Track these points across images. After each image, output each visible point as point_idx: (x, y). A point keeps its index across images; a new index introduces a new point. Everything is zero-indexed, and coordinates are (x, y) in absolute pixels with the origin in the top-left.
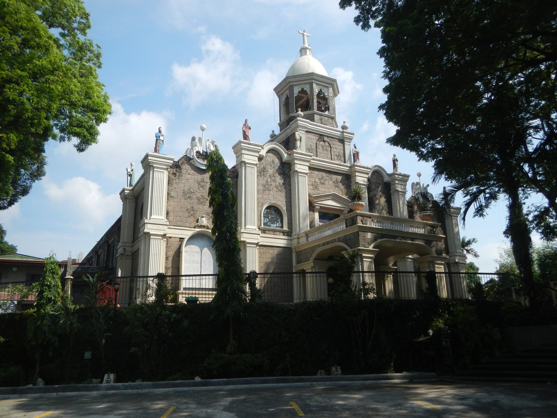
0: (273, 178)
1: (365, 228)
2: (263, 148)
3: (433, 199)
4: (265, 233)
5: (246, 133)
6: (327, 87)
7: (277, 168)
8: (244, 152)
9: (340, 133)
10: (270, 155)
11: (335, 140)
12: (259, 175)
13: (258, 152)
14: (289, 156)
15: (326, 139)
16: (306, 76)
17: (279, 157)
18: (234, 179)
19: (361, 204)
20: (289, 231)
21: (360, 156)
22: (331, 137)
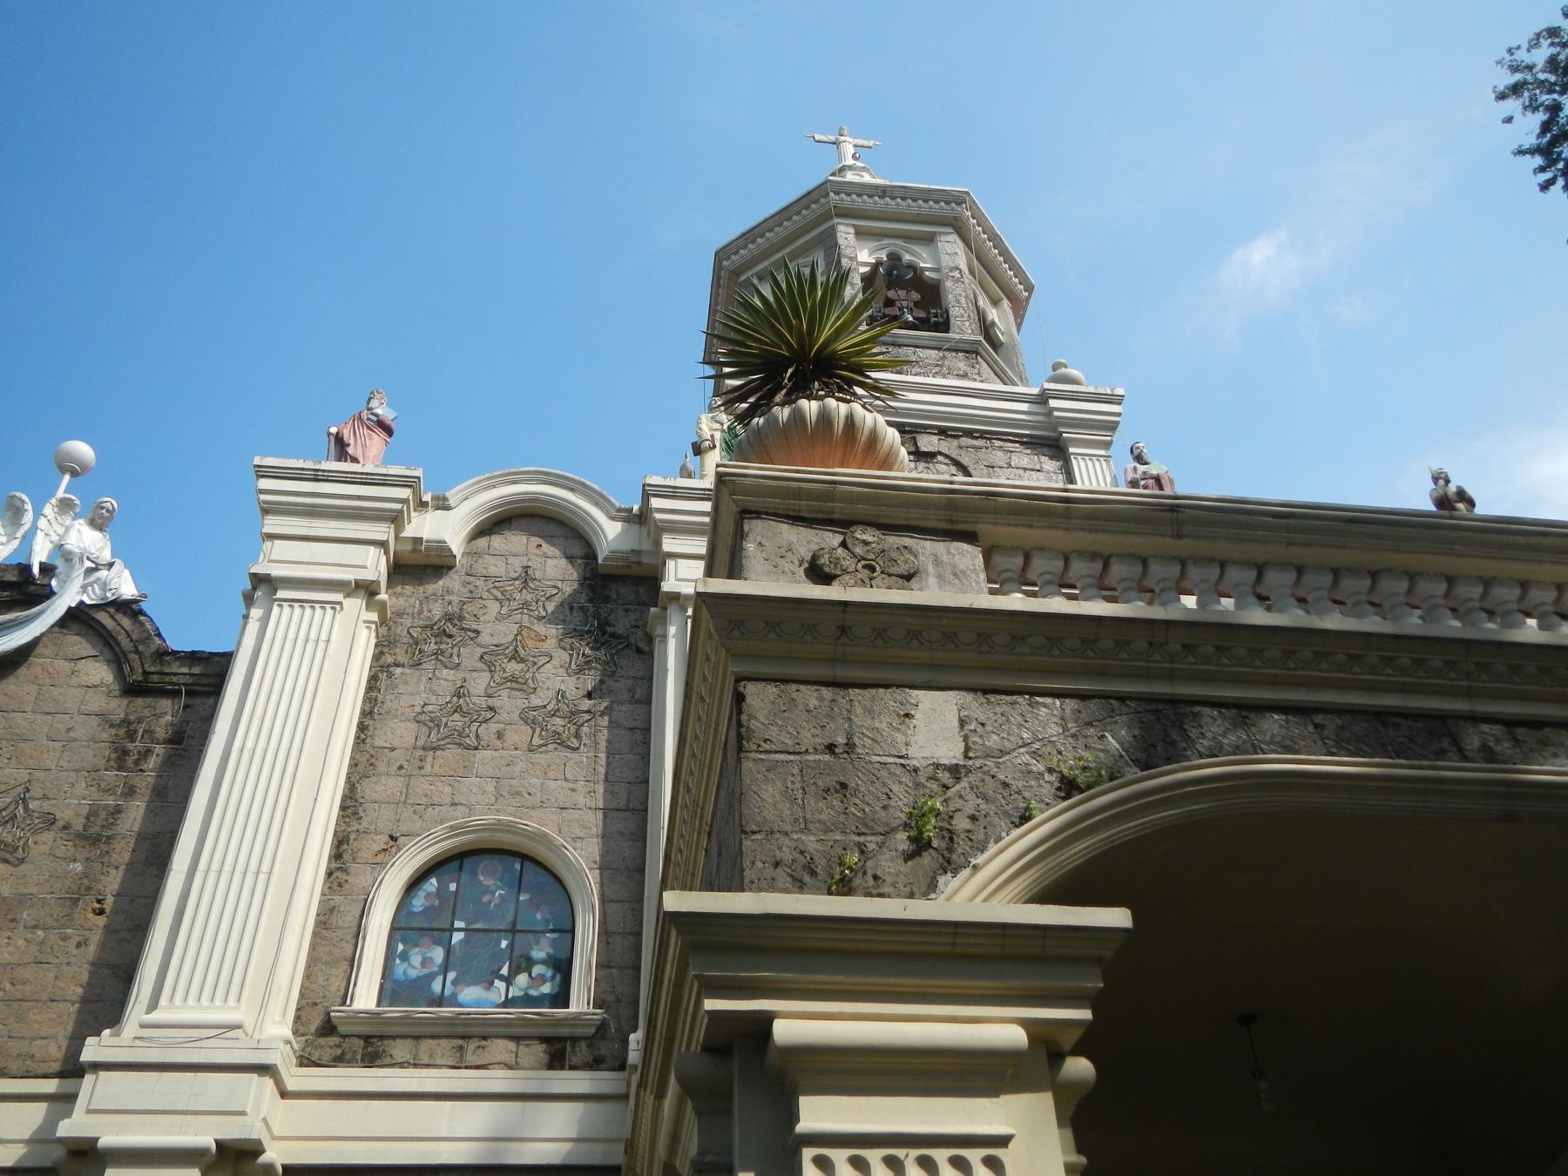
0: (513, 667)
1: (843, 630)
2: (442, 504)
4: (372, 1059)
5: (350, 450)
6: (929, 240)
7: (551, 607)
8: (273, 524)
9: (1024, 407)
10: (516, 544)
11: (998, 443)
12: (402, 659)
13: (396, 519)
14: (635, 527)
16: (799, 213)
17: (577, 549)
18: (197, 701)
19: (825, 417)
20: (602, 1027)
22: (969, 433)
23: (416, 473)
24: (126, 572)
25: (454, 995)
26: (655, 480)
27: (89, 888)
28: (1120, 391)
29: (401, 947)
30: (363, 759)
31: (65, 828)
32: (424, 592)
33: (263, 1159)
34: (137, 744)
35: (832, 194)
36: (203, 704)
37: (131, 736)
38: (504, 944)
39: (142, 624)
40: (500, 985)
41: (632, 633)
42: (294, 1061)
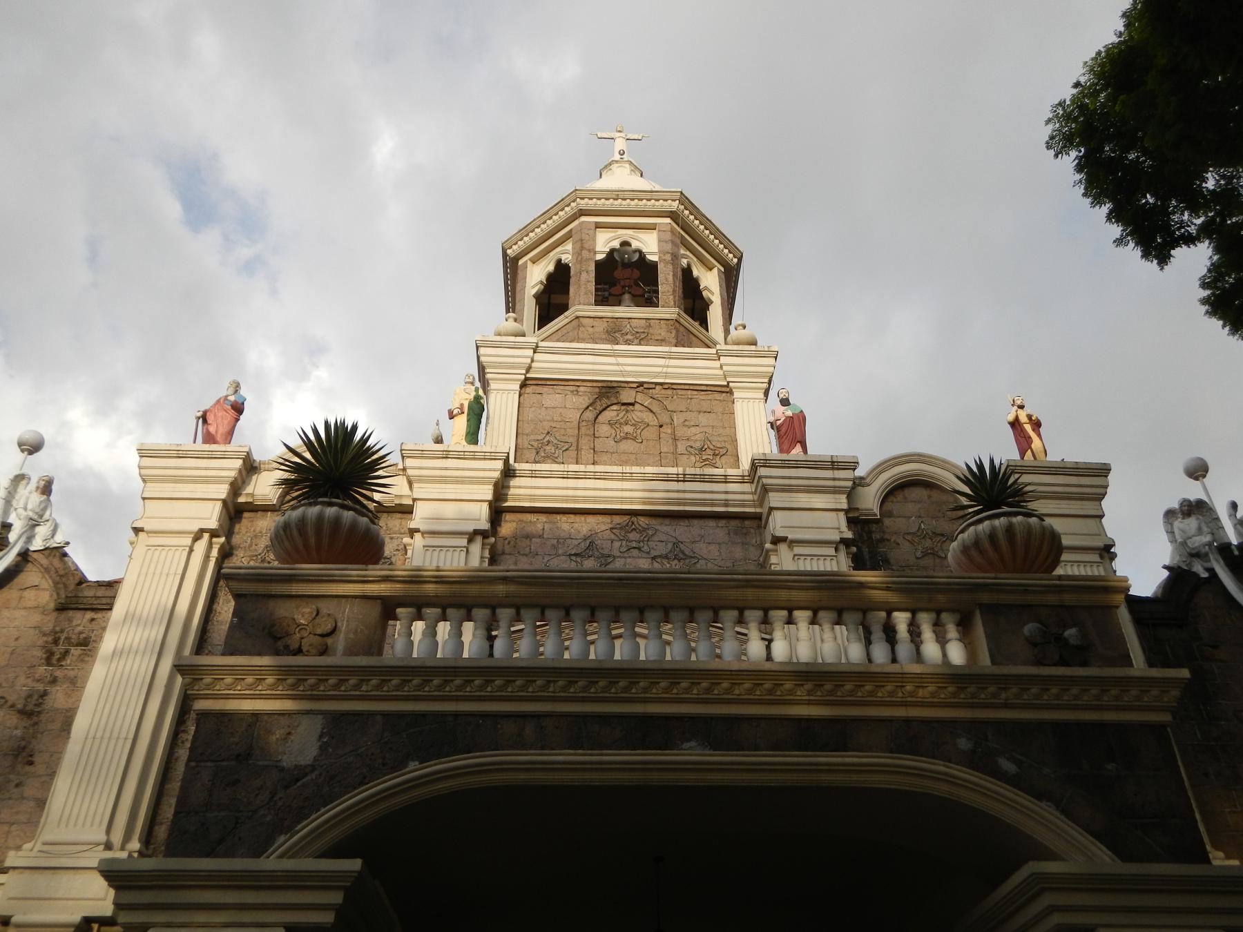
15: (627, 396)
18: (98, 615)
27: (24, 748)
31: (13, 706)
32: (254, 531)
34: (58, 647)
35: (578, 200)
36: (104, 617)
37: (56, 642)
39: (65, 563)
41: (394, 555)
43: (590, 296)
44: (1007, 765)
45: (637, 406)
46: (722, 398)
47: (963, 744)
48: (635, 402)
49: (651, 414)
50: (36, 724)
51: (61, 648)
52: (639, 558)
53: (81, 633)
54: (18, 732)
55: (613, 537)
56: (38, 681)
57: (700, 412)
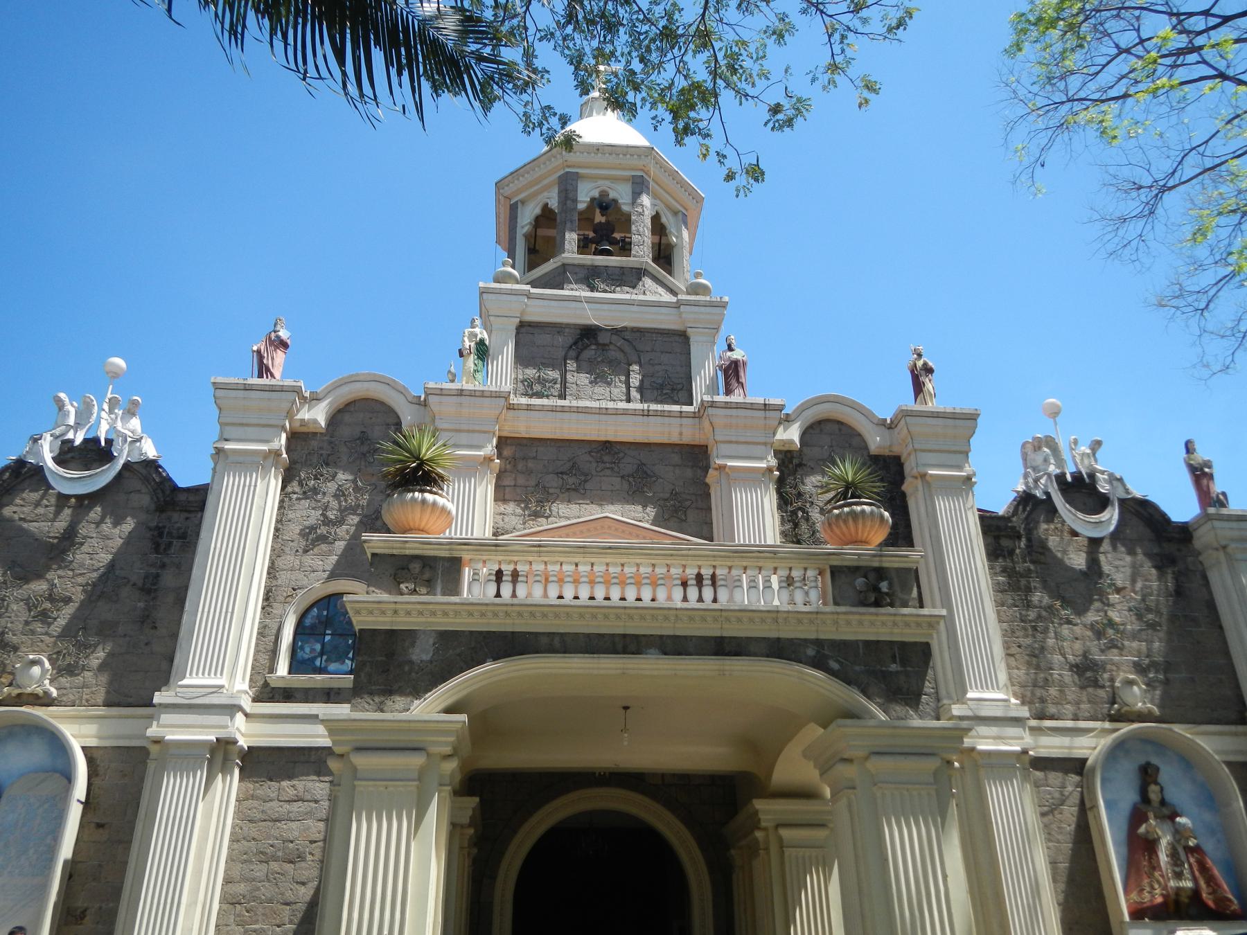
3: (1127, 491)
5: (265, 361)
15: (603, 338)
18: (192, 515)
21: (747, 377)
23: (298, 384)
24: (149, 441)
25: (326, 667)
26: (431, 385)
27: (148, 616)
28: (726, 299)
29: (300, 644)
30: (277, 546)
31: (134, 585)
33: (239, 744)
37: (161, 535)
38: (350, 641)
39: (160, 473)
40: (348, 662)
42: (250, 700)
43: (573, 243)
44: (834, 665)
45: (612, 347)
46: (680, 340)
47: (811, 652)
48: (611, 343)
49: (622, 354)
50: (154, 598)
51: (165, 539)
52: (611, 476)
53: (179, 529)
54: (141, 605)
55: (591, 459)
56: (151, 565)
57: (662, 352)
